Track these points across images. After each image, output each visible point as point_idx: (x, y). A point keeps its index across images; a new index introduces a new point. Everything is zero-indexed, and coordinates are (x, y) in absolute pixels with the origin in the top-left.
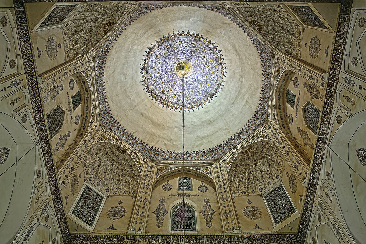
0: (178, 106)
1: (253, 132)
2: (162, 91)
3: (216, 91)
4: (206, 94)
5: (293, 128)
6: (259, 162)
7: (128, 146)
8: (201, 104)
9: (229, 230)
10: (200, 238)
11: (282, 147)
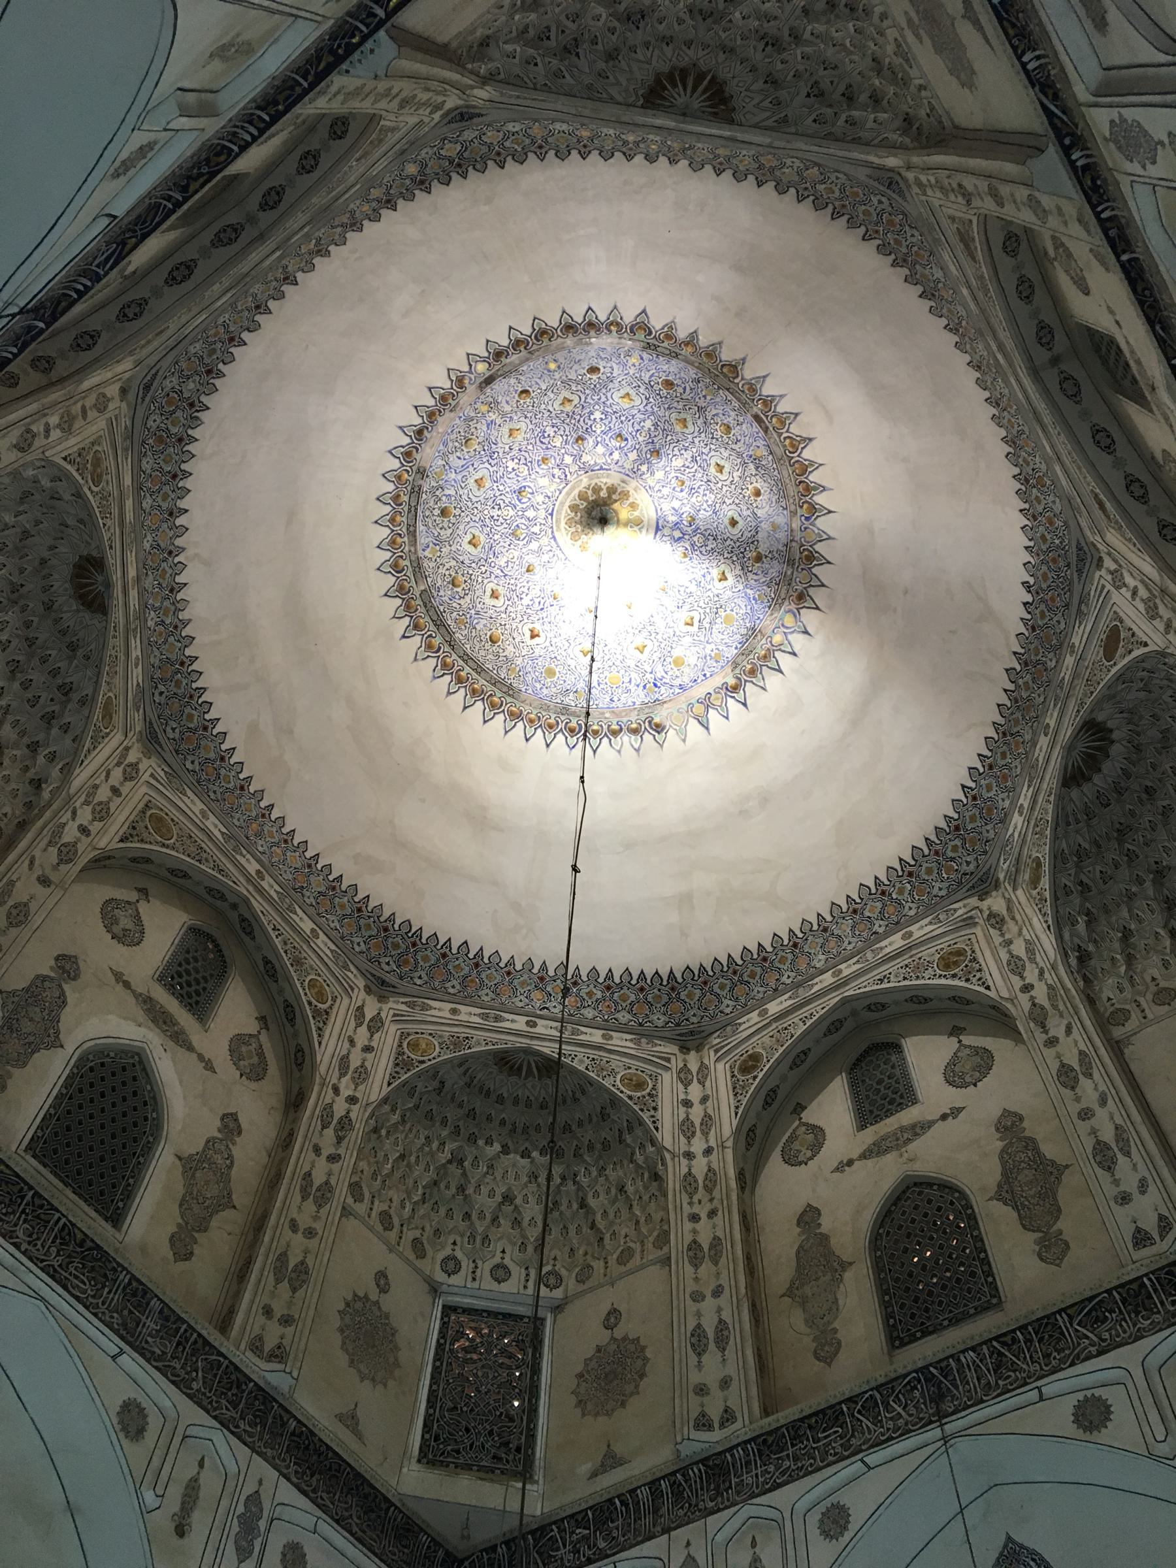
0: (432, 628)
1: (607, 1027)
2: (444, 512)
3: (615, 733)
5: (785, 1187)
6: (525, 1154)
7: (133, 594)
8: (511, 714)
9: (256, 1346)
10: (134, 1295)
11: (687, 1209)
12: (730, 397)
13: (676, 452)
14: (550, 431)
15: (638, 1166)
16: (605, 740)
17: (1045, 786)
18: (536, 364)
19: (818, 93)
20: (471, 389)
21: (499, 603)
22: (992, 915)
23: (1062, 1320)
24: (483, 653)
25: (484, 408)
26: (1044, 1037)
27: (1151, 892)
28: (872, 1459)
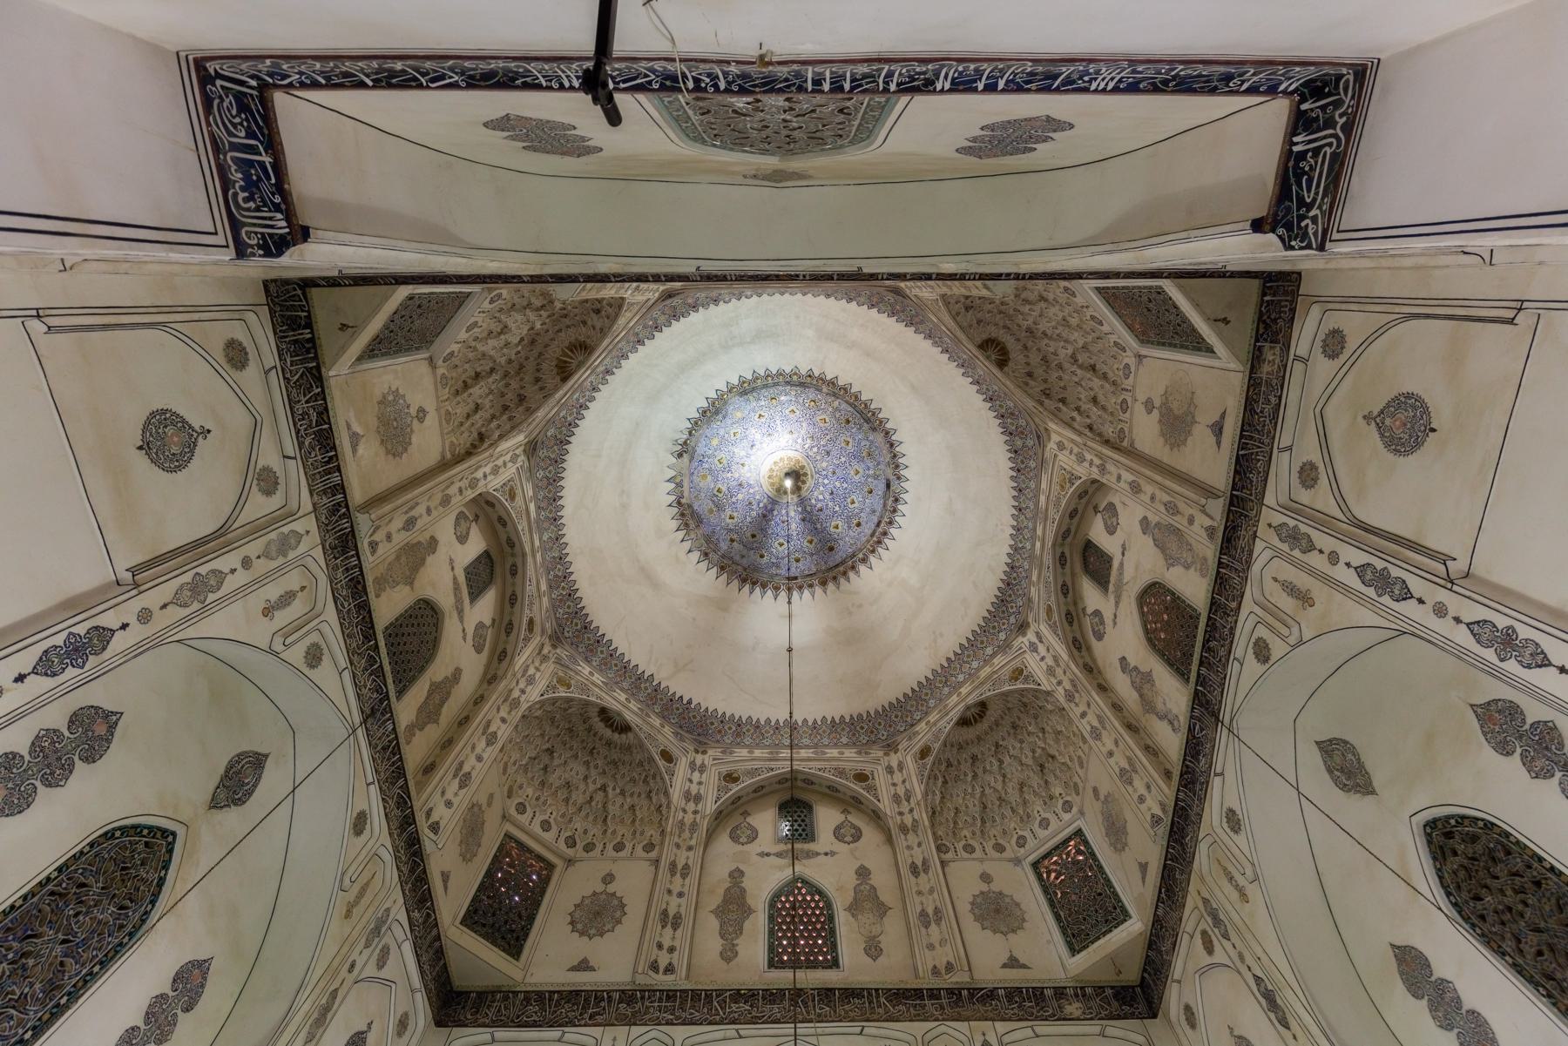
4: (720, 417)
18: (879, 508)
20: (892, 478)
28: (347, 675)
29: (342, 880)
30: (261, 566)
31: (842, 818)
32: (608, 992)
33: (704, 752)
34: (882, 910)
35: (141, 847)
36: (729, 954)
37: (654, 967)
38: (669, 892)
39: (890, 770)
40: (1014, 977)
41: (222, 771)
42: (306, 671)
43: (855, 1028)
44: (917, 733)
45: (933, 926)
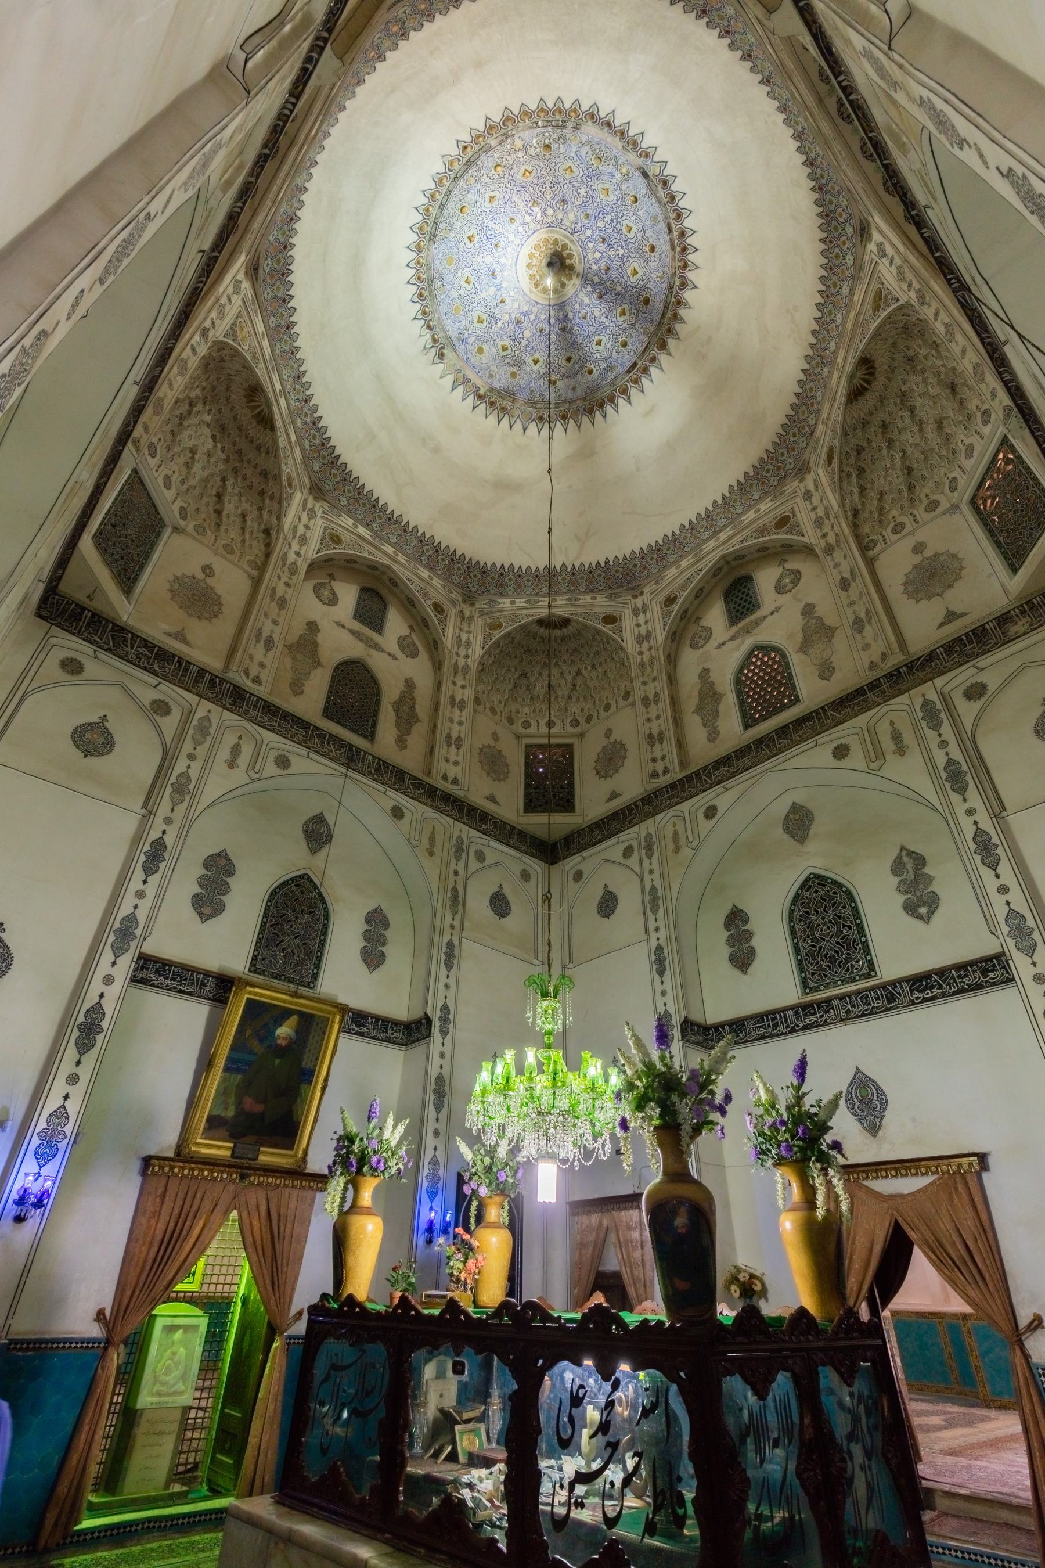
0: (465, 160)
3: (429, 328)
4: (438, 283)
12: (645, 345)
13: (604, 310)
14: (608, 218)
15: (261, 516)
16: (423, 322)
17: (532, 611)
18: (656, 209)
19: (859, 451)
20: (640, 161)
21: (488, 205)
22: (461, 612)
23: (407, 777)
24: (453, 205)
25: (624, 171)
26: (452, 678)
27: (516, 677)
28: (313, 755)
29: (410, 844)
30: (201, 751)
31: (781, 569)
32: (634, 804)
33: (642, 593)
34: (827, 632)
35: (295, 888)
36: (713, 735)
37: (655, 775)
38: (649, 720)
39: (808, 496)
40: (954, 629)
41: (302, 836)
42: (285, 772)
43: (811, 743)
44: (819, 439)
45: (868, 628)
